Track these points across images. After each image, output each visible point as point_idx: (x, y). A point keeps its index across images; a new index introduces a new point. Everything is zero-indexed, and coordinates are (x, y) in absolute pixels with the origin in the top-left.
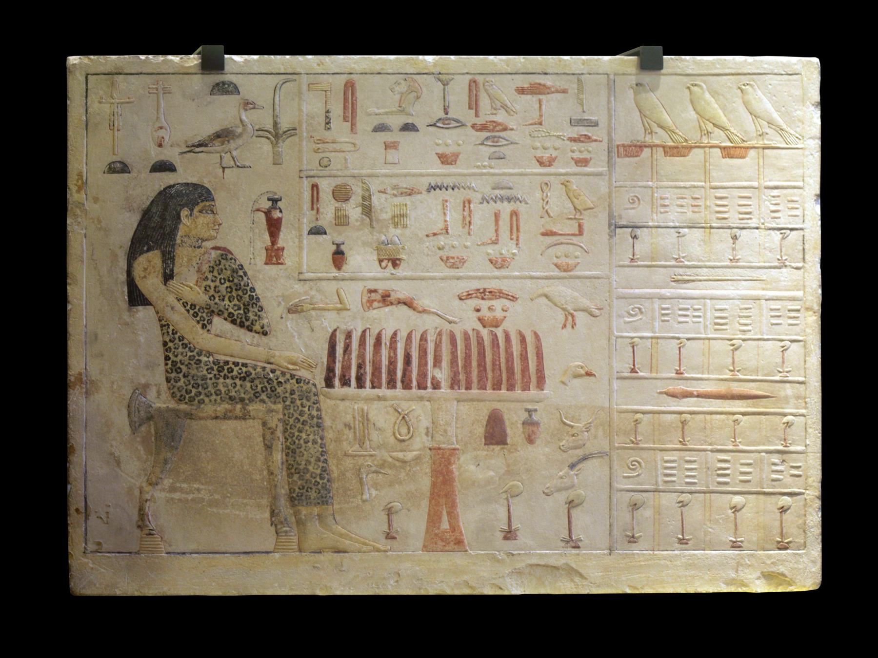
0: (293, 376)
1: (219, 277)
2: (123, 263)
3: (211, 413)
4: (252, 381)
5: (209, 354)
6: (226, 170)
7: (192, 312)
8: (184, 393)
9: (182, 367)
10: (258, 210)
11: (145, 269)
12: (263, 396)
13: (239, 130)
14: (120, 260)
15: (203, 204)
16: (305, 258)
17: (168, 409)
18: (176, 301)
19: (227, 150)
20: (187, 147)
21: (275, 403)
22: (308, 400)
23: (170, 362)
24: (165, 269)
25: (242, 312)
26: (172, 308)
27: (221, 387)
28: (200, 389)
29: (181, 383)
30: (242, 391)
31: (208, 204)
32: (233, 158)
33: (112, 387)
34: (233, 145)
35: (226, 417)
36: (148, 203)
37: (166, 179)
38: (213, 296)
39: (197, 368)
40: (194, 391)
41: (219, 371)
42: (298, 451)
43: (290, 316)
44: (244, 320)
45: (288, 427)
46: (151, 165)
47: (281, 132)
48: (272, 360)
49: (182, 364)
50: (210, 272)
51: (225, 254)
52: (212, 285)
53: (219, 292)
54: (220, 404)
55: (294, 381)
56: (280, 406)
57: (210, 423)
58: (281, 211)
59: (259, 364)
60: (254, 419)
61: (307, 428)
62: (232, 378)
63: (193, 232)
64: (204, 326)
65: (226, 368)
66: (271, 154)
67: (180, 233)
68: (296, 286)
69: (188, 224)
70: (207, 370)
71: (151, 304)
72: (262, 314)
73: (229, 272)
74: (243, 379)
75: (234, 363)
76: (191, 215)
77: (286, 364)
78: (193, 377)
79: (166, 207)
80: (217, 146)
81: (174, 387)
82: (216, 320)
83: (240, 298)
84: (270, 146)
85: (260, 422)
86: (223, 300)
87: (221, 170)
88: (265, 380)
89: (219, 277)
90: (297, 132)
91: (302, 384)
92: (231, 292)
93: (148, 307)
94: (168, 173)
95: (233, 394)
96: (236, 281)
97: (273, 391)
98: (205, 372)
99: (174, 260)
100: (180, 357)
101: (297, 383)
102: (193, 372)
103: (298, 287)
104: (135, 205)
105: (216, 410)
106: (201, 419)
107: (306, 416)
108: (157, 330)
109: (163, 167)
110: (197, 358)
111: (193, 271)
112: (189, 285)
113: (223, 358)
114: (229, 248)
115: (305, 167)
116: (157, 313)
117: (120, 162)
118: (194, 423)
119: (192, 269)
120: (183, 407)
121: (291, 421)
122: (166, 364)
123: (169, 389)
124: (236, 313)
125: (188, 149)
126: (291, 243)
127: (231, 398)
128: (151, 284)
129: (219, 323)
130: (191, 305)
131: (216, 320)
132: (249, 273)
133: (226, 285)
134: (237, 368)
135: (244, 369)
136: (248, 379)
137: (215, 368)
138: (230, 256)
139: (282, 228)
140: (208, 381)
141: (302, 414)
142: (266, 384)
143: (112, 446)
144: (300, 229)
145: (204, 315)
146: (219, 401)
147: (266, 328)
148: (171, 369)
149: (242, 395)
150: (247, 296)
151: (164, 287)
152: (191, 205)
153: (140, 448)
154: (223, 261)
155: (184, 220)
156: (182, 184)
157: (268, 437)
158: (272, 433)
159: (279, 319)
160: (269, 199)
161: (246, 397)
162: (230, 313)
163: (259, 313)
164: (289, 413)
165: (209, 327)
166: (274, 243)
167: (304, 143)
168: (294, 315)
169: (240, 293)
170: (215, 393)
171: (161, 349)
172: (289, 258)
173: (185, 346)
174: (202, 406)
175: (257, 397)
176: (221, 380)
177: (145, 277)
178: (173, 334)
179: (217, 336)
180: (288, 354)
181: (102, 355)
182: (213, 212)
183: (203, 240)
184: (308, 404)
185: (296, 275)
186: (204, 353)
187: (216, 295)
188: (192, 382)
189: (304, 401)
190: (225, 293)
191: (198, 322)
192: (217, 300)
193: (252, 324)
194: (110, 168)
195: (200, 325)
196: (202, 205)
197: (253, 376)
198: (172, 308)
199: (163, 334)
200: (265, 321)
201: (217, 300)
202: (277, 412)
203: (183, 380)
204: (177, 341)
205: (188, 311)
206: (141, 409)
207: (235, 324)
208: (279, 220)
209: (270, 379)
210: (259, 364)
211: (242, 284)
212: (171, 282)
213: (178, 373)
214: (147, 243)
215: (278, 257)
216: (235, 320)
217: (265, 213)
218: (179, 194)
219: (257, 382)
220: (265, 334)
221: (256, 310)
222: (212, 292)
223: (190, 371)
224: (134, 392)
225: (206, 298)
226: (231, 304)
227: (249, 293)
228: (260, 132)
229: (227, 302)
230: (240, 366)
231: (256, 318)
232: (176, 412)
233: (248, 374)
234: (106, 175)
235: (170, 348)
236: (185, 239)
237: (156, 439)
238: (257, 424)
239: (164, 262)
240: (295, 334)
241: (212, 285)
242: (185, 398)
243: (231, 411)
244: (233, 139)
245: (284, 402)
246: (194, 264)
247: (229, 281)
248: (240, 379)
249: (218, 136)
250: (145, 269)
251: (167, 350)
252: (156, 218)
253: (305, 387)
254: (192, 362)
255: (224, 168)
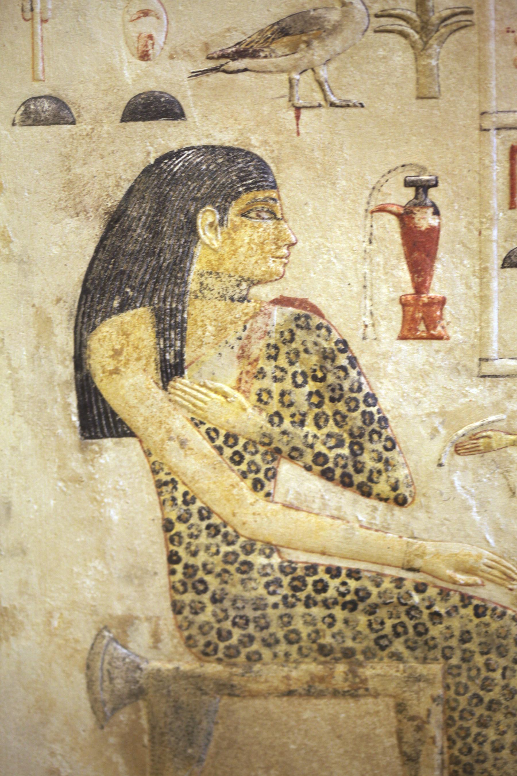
0: (466, 600)
1: (291, 370)
2: (64, 339)
3: (276, 683)
4: (372, 611)
5: (271, 549)
6: (305, 114)
7: (228, 452)
8: (213, 636)
9: (208, 578)
10: (382, 209)
11: (117, 353)
12: (398, 645)
13: (334, 16)
14: (57, 331)
15: (251, 195)
16: (495, 324)
17: (178, 675)
18: (190, 426)
19: (303, 65)
20: (210, 58)
21: (425, 660)
22: (502, 655)
23: (179, 568)
24: (163, 352)
25: (345, 451)
26: (183, 444)
27: (298, 624)
28: (251, 629)
29: (206, 616)
30: (349, 634)
31: (261, 195)
32: (320, 84)
33: (49, 623)
34: (318, 52)
35: (311, 691)
36: (120, 195)
37: (161, 138)
38: (277, 414)
39: (243, 582)
40: (237, 634)
41: (295, 589)
42: (477, 767)
43: (460, 460)
44: (350, 470)
45: (456, 715)
46: (123, 104)
47: (434, 18)
48: (418, 563)
49: (209, 572)
50: (269, 357)
51: (306, 315)
52: (276, 388)
53: (291, 404)
54: (297, 662)
55: (469, 611)
56: (436, 669)
57: (275, 706)
58: (436, 213)
59: (388, 571)
60: (376, 695)
61: (499, 716)
62: (326, 604)
63: (228, 265)
64: (257, 485)
65: (310, 580)
66: (412, 74)
67: (197, 267)
68: (474, 391)
69: (216, 245)
70: (267, 585)
71: (132, 435)
72: (393, 455)
73: (314, 359)
74: (351, 606)
75: (328, 570)
76: (221, 222)
77: (449, 572)
78: (234, 602)
79: (161, 204)
80: (279, 56)
81: (191, 624)
82: (286, 469)
83: (340, 419)
84: (410, 54)
85: (391, 702)
86: (302, 423)
87: (292, 113)
88: (402, 609)
89: (291, 370)
90: (474, 18)
91: (487, 619)
92: (319, 405)
93: (125, 440)
94: (163, 122)
95: (327, 640)
96: (331, 379)
97: (419, 634)
98: (262, 591)
99: (184, 330)
100: (202, 557)
101: (477, 615)
102: (235, 590)
103: (478, 392)
104: (88, 200)
105: (287, 678)
106: (254, 695)
107: (497, 689)
108: (149, 495)
109: (153, 108)
110: (242, 557)
111: (230, 355)
112: (222, 390)
113: (302, 558)
114: (313, 300)
115: (493, 106)
116: (148, 454)
117: (49, 97)
118: (238, 704)
119: (226, 351)
120: (212, 668)
121: (463, 701)
122: (173, 572)
123: (180, 627)
124: (331, 455)
125: (212, 64)
126: (461, 289)
127: (324, 651)
128: (131, 388)
129: (291, 476)
130: (227, 436)
131: (286, 469)
132: (362, 361)
133: (307, 389)
134: (336, 582)
135: (353, 584)
136: (361, 606)
137: (286, 580)
138: (316, 320)
139: (440, 254)
140: (270, 611)
141: (487, 685)
142: (404, 618)
143: (53, 754)
144: (482, 256)
145: (258, 458)
146: (295, 655)
147: (403, 490)
148: (184, 584)
149: (349, 643)
150: (357, 414)
151: (161, 394)
152: (223, 198)
153: (117, 758)
154: (300, 334)
155: (205, 234)
156: (199, 148)
157: (410, 736)
158: (419, 729)
159: (433, 467)
160: (408, 184)
161: (358, 647)
162: (319, 454)
163: (386, 454)
164: (458, 684)
165: (269, 486)
166: (420, 288)
167: (492, 46)
168: (469, 459)
169: (341, 406)
170: (286, 637)
171: (159, 536)
172: (455, 322)
173: (214, 530)
174: (257, 667)
175: (383, 648)
176: (300, 609)
177: (116, 371)
178: (185, 502)
179: (289, 506)
180: (456, 548)
181: (24, 552)
182: (273, 215)
183: (252, 283)
184: (503, 662)
185: (474, 364)
186: (259, 546)
187: (286, 413)
188: (232, 613)
189: (493, 656)
190: (305, 408)
191: (244, 475)
192: (287, 424)
193: (370, 479)
194: (27, 114)
195: (249, 482)
196: (246, 198)
197: (374, 599)
198: (183, 444)
199: (163, 503)
200: (401, 474)
201: (287, 424)
202: (429, 682)
203: (210, 608)
204: (195, 520)
205: (219, 449)
206: (116, 673)
207: (331, 479)
208: (433, 233)
209: (414, 607)
210: (388, 571)
211: (346, 386)
212: (178, 383)
213: (199, 593)
214: (120, 291)
215: (431, 322)
216: (331, 470)
217: (398, 215)
218: (192, 173)
219: (382, 613)
220: (401, 502)
221: (379, 447)
222: (274, 406)
223: (228, 587)
224: (99, 635)
225: (262, 419)
226: (322, 433)
227: (362, 407)
228: (384, 21)
229: (310, 428)
230: (343, 577)
231: (380, 466)
232: (197, 682)
233: (362, 595)
234: (18, 129)
235: (178, 534)
236: (210, 281)
237: (152, 740)
238: (383, 707)
239: (160, 334)
240: (472, 502)
241: (276, 388)
242: (216, 650)
243: (322, 679)
244: (318, 37)
245: (447, 658)
246: (232, 340)
247: (315, 378)
248: (344, 606)
249: (282, 30)
250: (117, 353)
251: (172, 540)
252: (139, 231)
253: (494, 626)
254: (232, 569)
255: (298, 109)
